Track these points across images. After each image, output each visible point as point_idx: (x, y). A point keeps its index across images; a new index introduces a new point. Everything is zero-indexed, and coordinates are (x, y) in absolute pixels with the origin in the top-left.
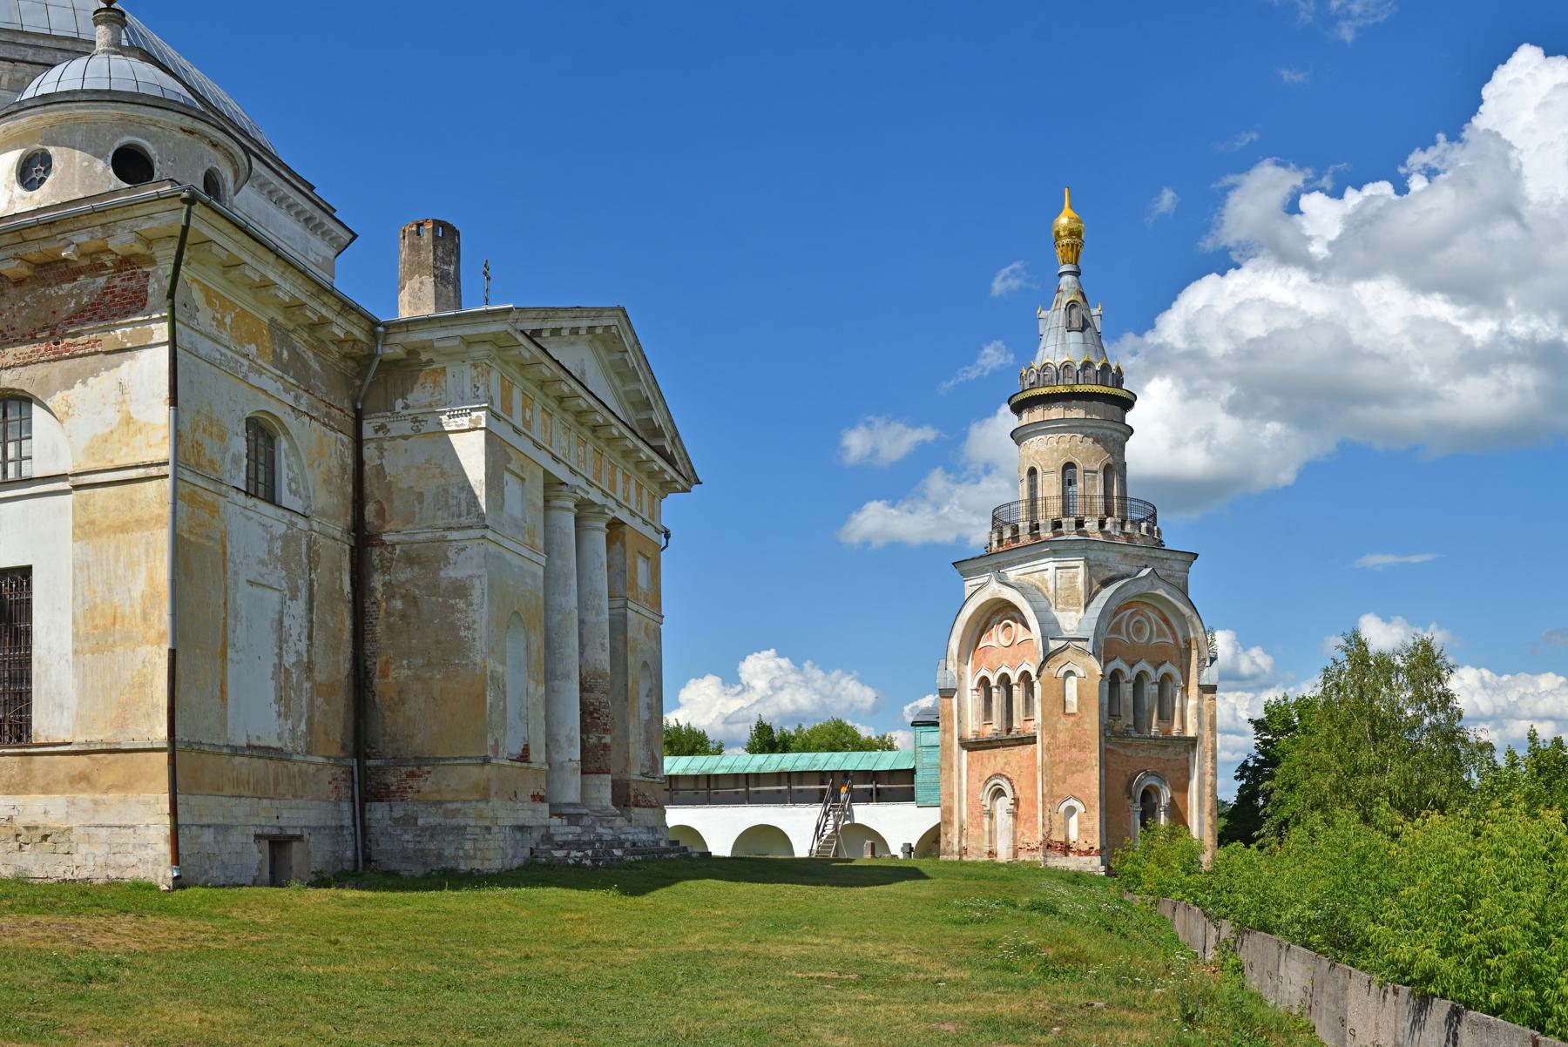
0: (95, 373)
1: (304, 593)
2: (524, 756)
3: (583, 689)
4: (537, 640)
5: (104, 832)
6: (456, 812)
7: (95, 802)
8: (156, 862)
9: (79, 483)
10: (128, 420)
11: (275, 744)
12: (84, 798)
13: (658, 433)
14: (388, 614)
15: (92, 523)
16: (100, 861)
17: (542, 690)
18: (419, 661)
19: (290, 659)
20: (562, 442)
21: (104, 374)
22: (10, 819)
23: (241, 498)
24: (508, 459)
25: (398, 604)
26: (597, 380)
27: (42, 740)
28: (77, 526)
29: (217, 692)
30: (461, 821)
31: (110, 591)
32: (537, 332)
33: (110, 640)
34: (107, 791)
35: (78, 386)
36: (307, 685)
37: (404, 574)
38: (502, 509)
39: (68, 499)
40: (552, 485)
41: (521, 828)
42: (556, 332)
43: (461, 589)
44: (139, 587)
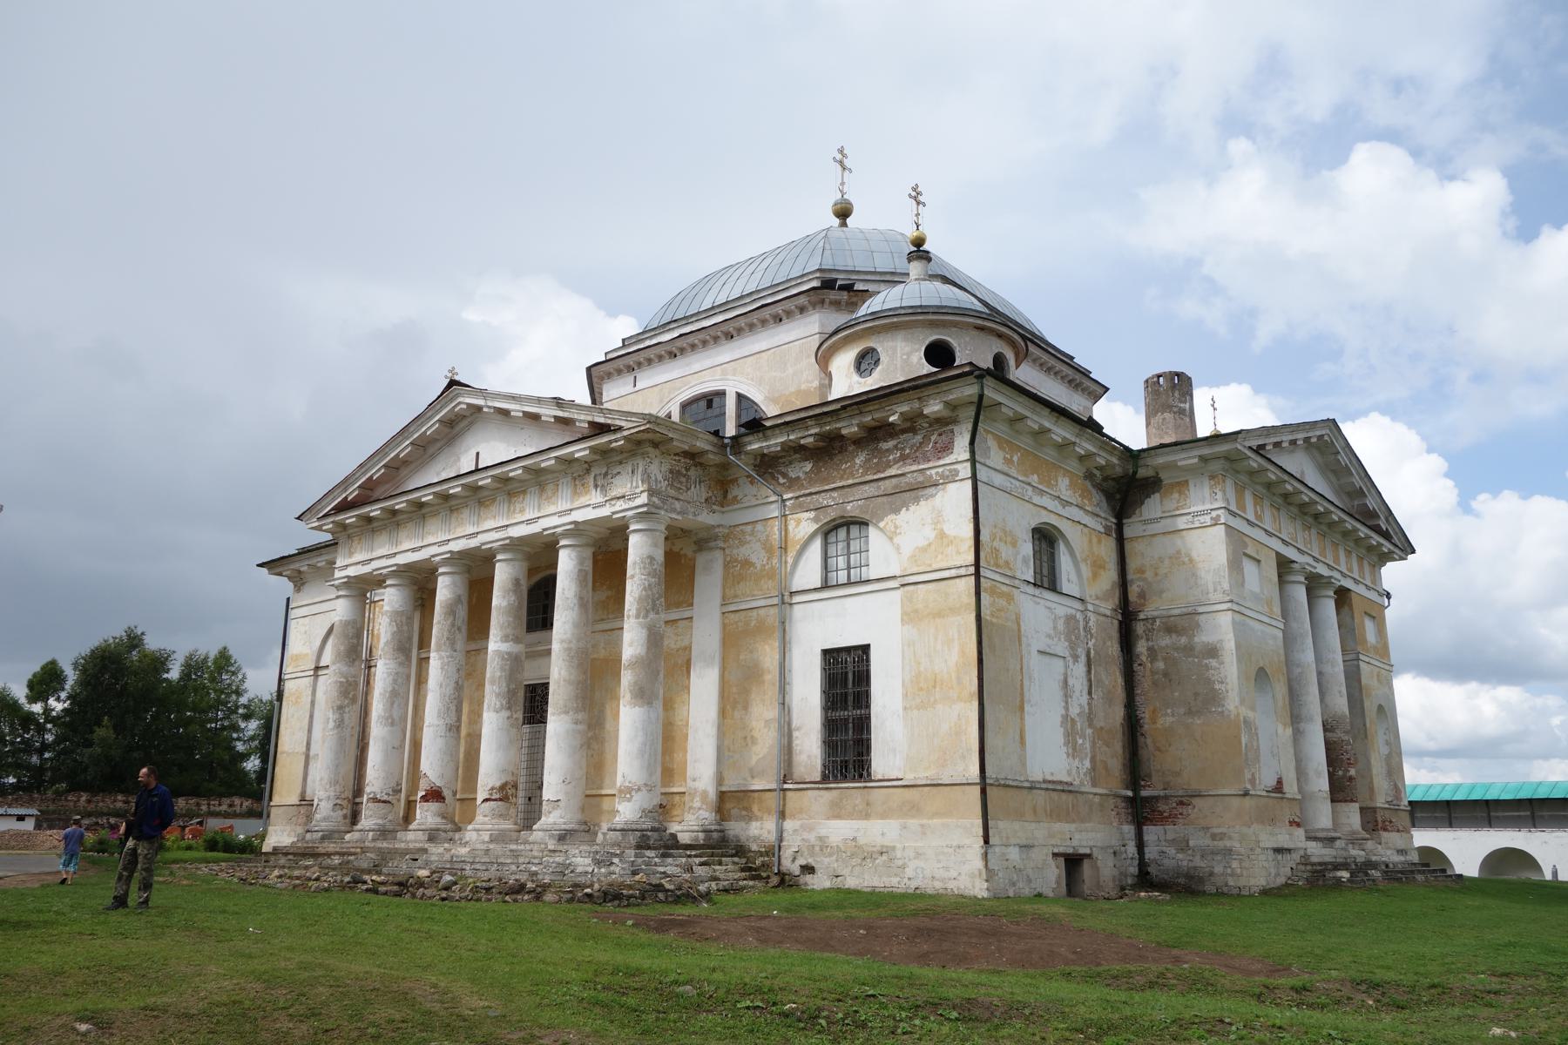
1: (1083, 659)
2: (1279, 787)
3: (1325, 730)
4: (1281, 690)
6: (1222, 836)
7: (922, 826)
8: (972, 876)
9: (905, 583)
10: (942, 535)
11: (1066, 779)
12: (913, 823)
13: (1373, 515)
14: (1153, 673)
15: (916, 611)
16: (928, 873)
17: (1289, 731)
18: (1182, 711)
19: (1074, 711)
20: (1288, 529)
22: (854, 839)
23: (1031, 589)
24: (1246, 546)
25: (1161, 665)
26: (1314, 479)
28: (904, 613)
29: (1017, 738)
30: (1228, 844)
32: (1262, 447)
34: (932, 817)
36: (1089, 731)
37: (1165, 641)
38: (1243, 585)
39: (897, 594)
40: (1284, 565)
41: (1278, 851)
42: (1277, 445)
43: (1213, 651)
44: (954, 657)
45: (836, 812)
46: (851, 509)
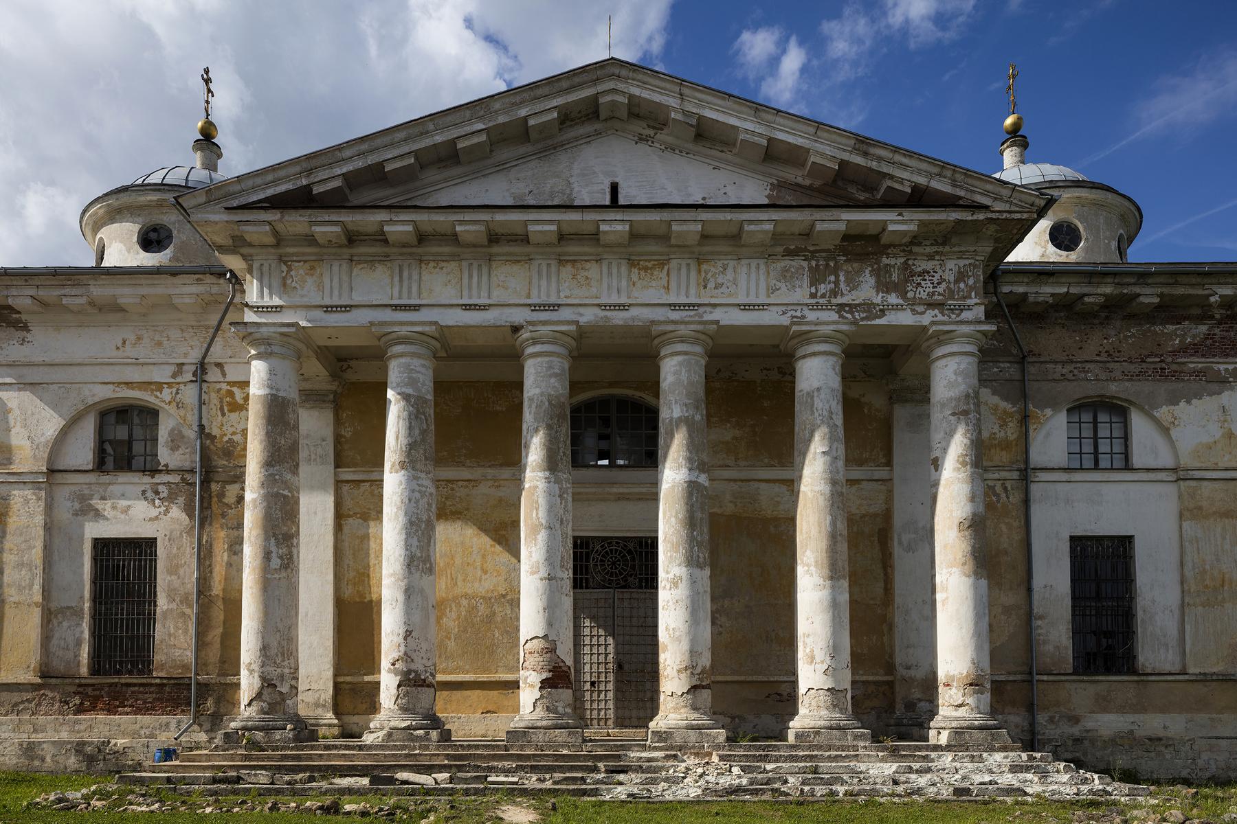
0: (1198, 396)
5: (1224, 743)
7: (1212, 720)
9: (1180, 474)
12: (1202, 717)
15: (1200, 508)
21: (1206, 399)
22: (1131, 732)
27: (1149, 671)
31: (1218, 560)
33: (1220, 598)
35: (1183, 404)
45: (1103, 704)
46: (1113, 389)
